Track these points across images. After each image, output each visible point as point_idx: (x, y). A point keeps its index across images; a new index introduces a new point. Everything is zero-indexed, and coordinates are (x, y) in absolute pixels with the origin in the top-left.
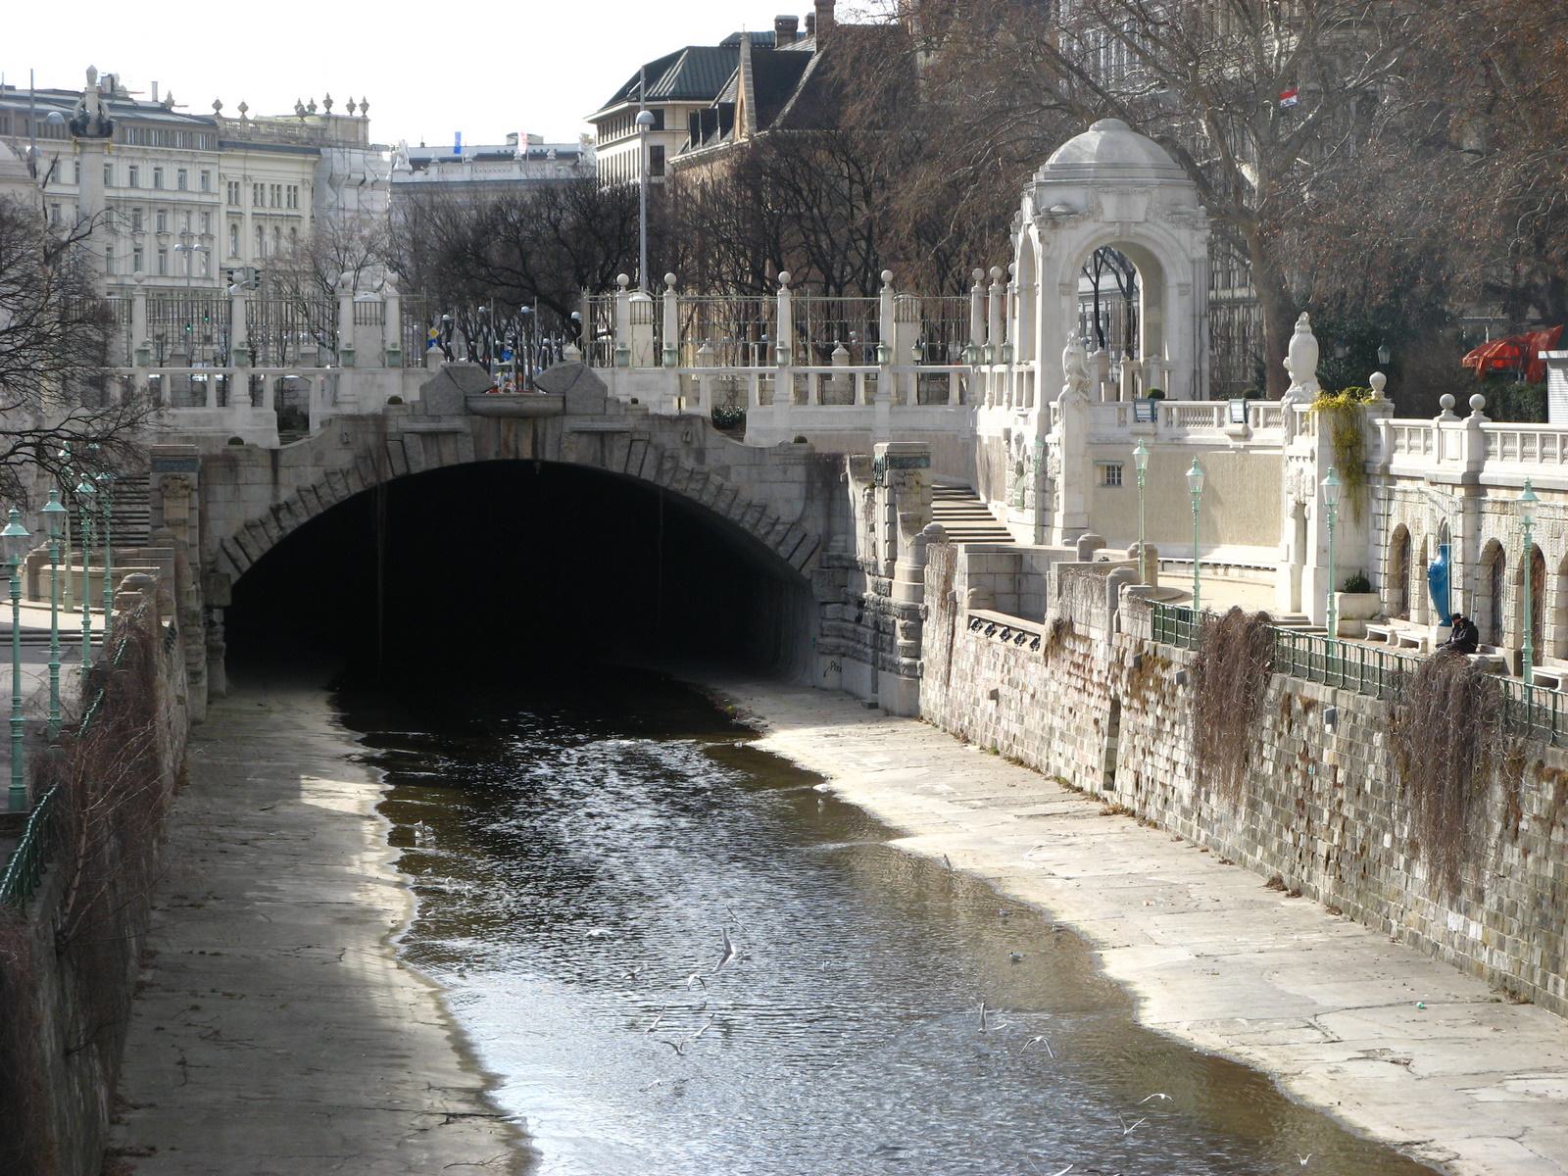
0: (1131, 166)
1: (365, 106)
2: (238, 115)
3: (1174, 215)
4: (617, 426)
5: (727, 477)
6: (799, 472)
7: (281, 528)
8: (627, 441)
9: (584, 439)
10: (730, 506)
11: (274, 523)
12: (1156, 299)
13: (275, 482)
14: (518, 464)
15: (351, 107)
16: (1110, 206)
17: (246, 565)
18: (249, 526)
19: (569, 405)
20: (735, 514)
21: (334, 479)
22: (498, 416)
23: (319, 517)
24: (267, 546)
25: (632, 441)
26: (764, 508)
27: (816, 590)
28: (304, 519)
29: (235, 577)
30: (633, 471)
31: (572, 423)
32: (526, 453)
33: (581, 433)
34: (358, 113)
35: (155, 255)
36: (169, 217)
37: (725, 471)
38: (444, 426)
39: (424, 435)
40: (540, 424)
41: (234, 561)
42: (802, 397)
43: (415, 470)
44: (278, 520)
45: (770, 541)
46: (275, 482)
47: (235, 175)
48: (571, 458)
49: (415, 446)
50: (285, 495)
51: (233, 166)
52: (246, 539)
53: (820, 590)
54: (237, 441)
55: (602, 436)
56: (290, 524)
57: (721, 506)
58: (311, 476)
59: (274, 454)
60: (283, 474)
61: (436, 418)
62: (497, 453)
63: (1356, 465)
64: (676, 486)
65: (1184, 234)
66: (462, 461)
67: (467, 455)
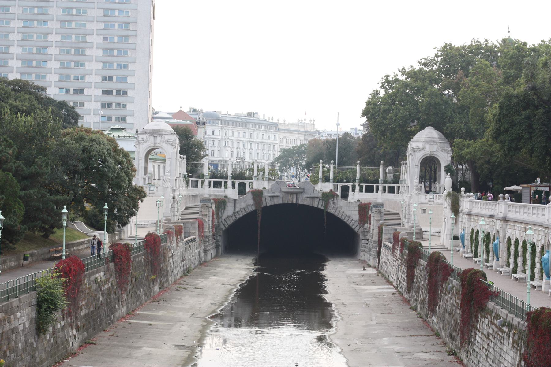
0: (433, 138)
1: (314, 121)
2: (283, 122)
3: (443, 150)
4: (316, 196)
5: (341, 209)
6: (357, 208)
8: (318, 200)
9: (308, 199)
12: (440, 170)
13: (235, 206)
15: (311, 121)
16: (428, 147)
17: (227, 226)
18: (228, 217)
20: (343, 218)
22: (287, 193)
24: (232, 222)
26: (350, 216)
27: (360, 236)
28: (241, 216)
29: (224, 229)
32: (294, 202)
33: (307, 197)
34: (312, 122)
35: (249, 154)
36: (266, 146)
37: (341, 207)
38: (276, 194)
39: (270, 197)
42: (361, 191)
43: (268, 205)
45: (351, 225)
46: (235, 206)
47: (282, 137)
48: (305, 203)
49: (268, 199)
50: (237, 210)
51: (282, 135)
52: (227, 220)
53: (361, 237)
54: (226, 197)
56: (238, 216)
57: (339, 216)
58: (243, 205)
59: (235, 200)
60: (237, 205)
61: (273, 193)
63: (455, 208)
65: (445, 154)
67: (280, 202)
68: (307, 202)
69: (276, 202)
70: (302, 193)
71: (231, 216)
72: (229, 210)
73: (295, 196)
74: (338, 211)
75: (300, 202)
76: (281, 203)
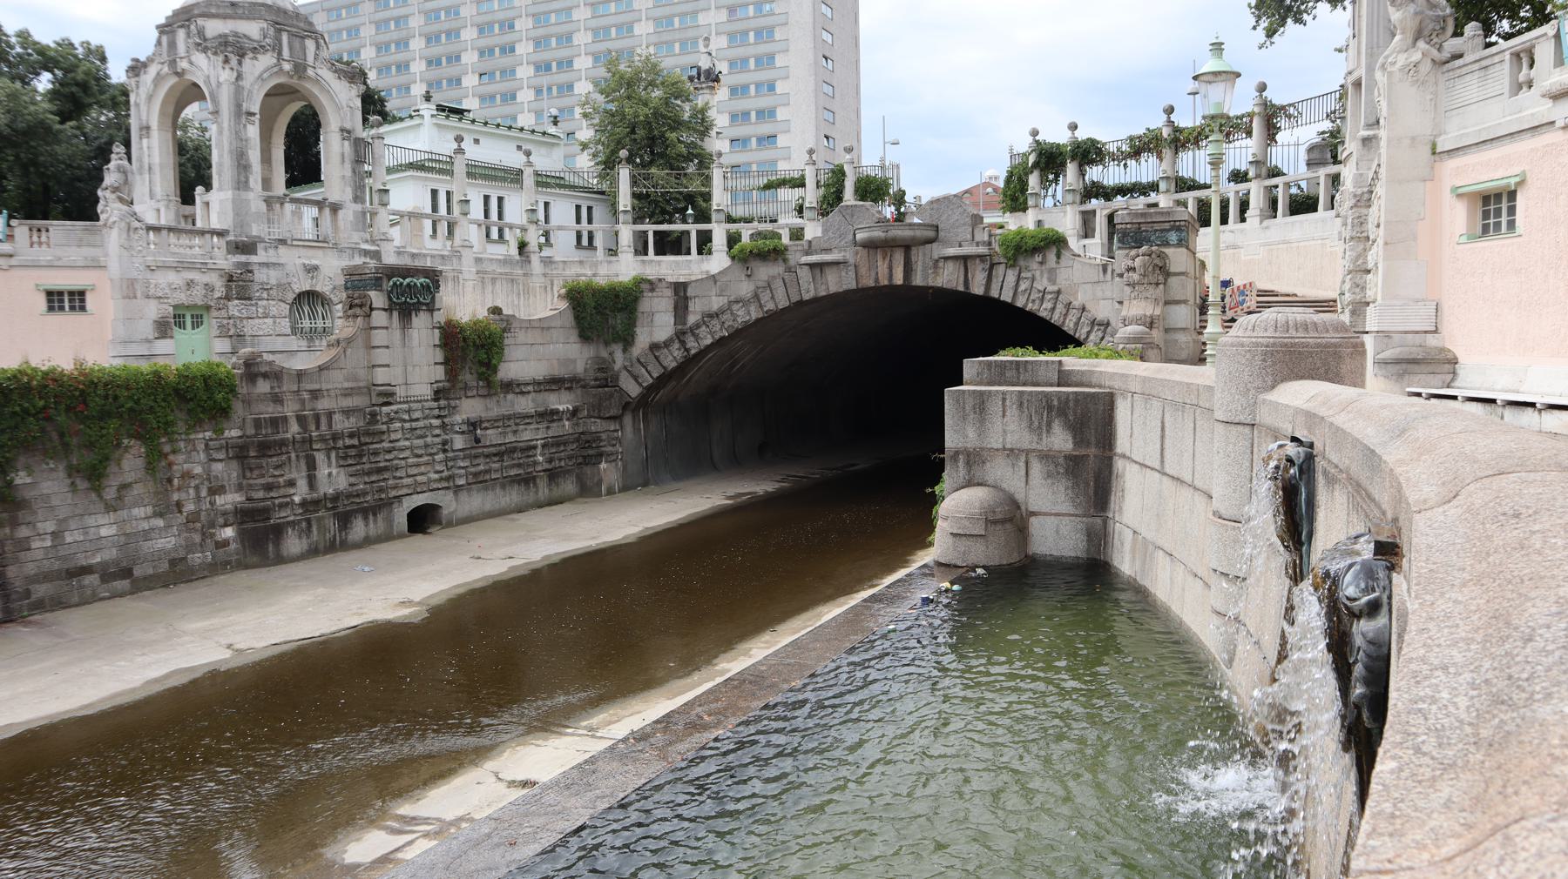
7: (687, 350)
9: (950, 265)
10: (1077, 324)
11: (677, 345)
14: (892, 288)
18: (654, 347)
19: (941, 234)
21: (735, 307)
22: (871, 246)
23: (722, 338)
25: (992, 266)
26: (1108, 324)
28: (709, 341)
29: (633, 390)
30: (994, 293)
31: (938, 250)
32: (899, 279)
33: (947, 258)
39: (812, 266)
40: (914, 251)
41: (636, 378)
43: (806, 297)
44: (683, 343)
55: (965, 260)
56: (693, 346)
62: (877, 280)
64: (1029, 307)
66: (845, 287)
68: (949, 278)
69: (835, 283)
70: (930, 241)
71: (667, 344)
72: (657, 323)
73: (899, 257)
74: (1060, 308)
75: (918, 280)
76: (853, 286)
